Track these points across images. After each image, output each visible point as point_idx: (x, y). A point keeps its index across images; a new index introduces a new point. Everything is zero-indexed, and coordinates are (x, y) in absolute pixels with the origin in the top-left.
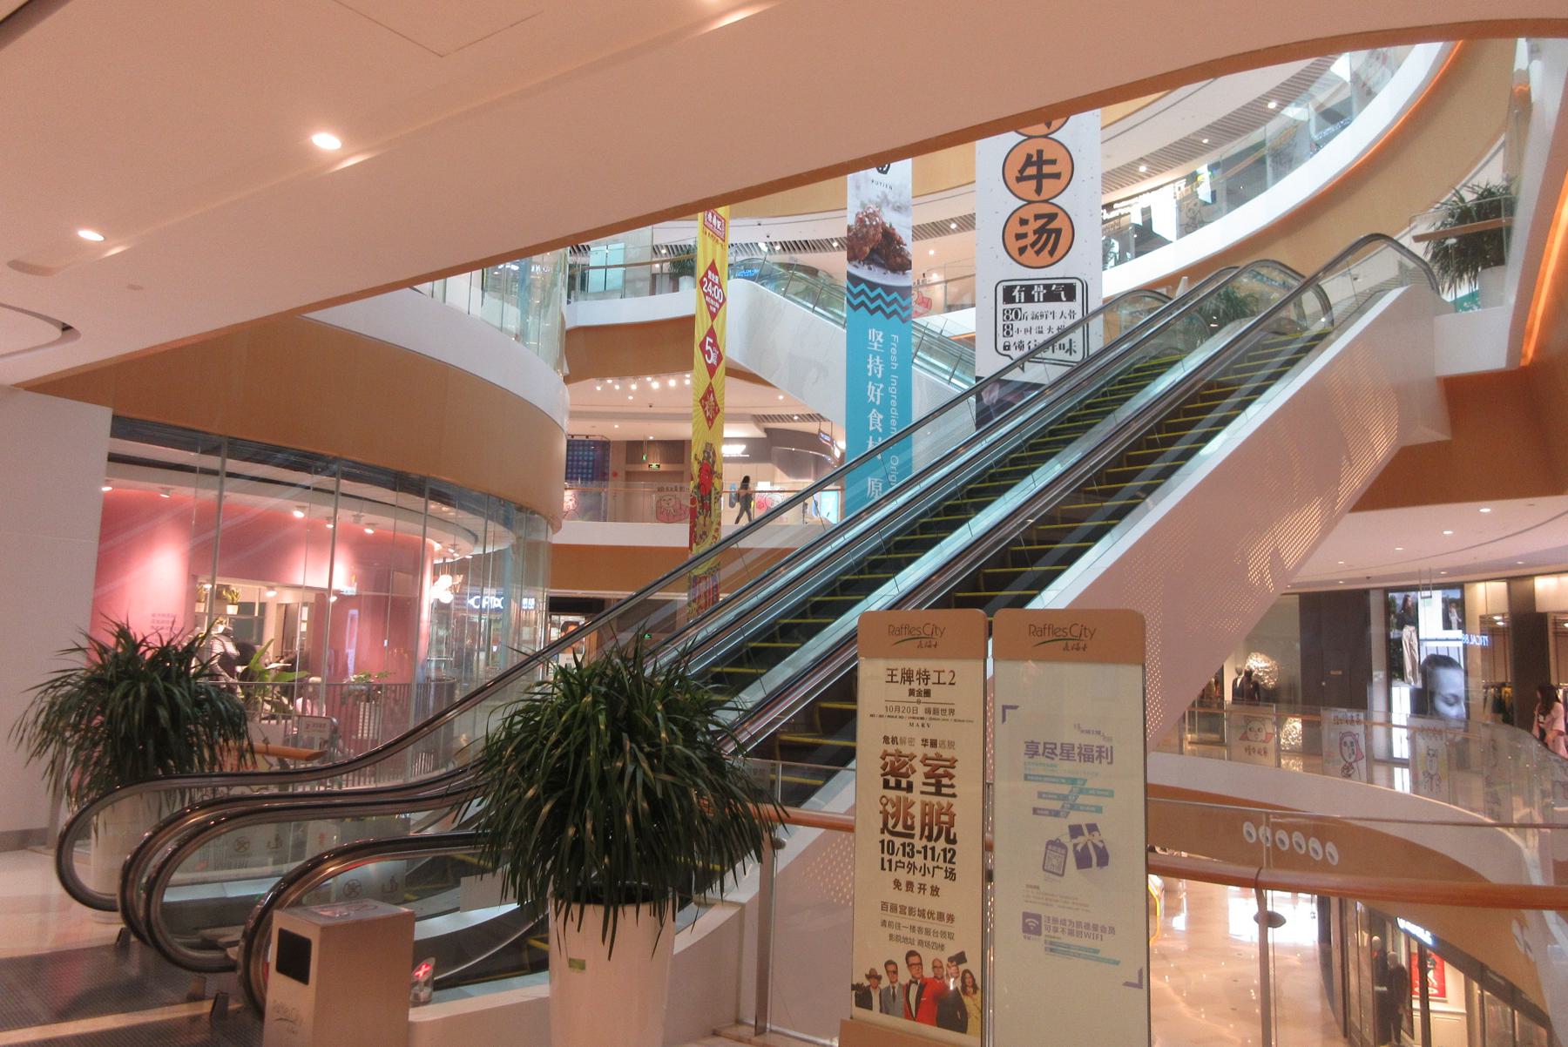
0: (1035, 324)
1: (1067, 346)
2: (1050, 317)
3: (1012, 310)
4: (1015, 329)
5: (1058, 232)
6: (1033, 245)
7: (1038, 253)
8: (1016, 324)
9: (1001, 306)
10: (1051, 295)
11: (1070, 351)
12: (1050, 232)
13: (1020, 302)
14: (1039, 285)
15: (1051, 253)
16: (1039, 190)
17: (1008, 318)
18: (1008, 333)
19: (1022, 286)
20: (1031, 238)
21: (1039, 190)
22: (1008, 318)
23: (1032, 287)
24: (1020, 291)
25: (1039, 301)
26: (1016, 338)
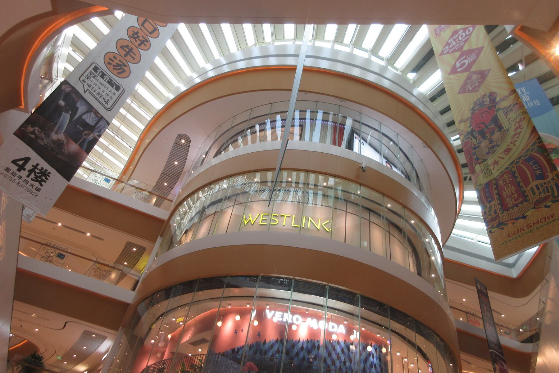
0: (99, 85)
1: (106, 100)
2: (106, 88)
3: (94, 74)
4: (91, 79)
5: (124, 71)
6: (114, 66)
7: (114, 69)
8: (92, 79)
9: (91, 69)
10: (110, 82)
11: (106, 102)
12: (121, 68)
13: (98, 75)
14: (108, 77)
15: (119, 73)
16: (125, 56)
17: (91, 74)
18: (88, 78)
19: (102, 71)
20: (114, 63)
21: (125, 56)
22: (91, 74)
23: (106, 75)
24: (100, 72)
25: (105, 80)
26: (90, 82)
